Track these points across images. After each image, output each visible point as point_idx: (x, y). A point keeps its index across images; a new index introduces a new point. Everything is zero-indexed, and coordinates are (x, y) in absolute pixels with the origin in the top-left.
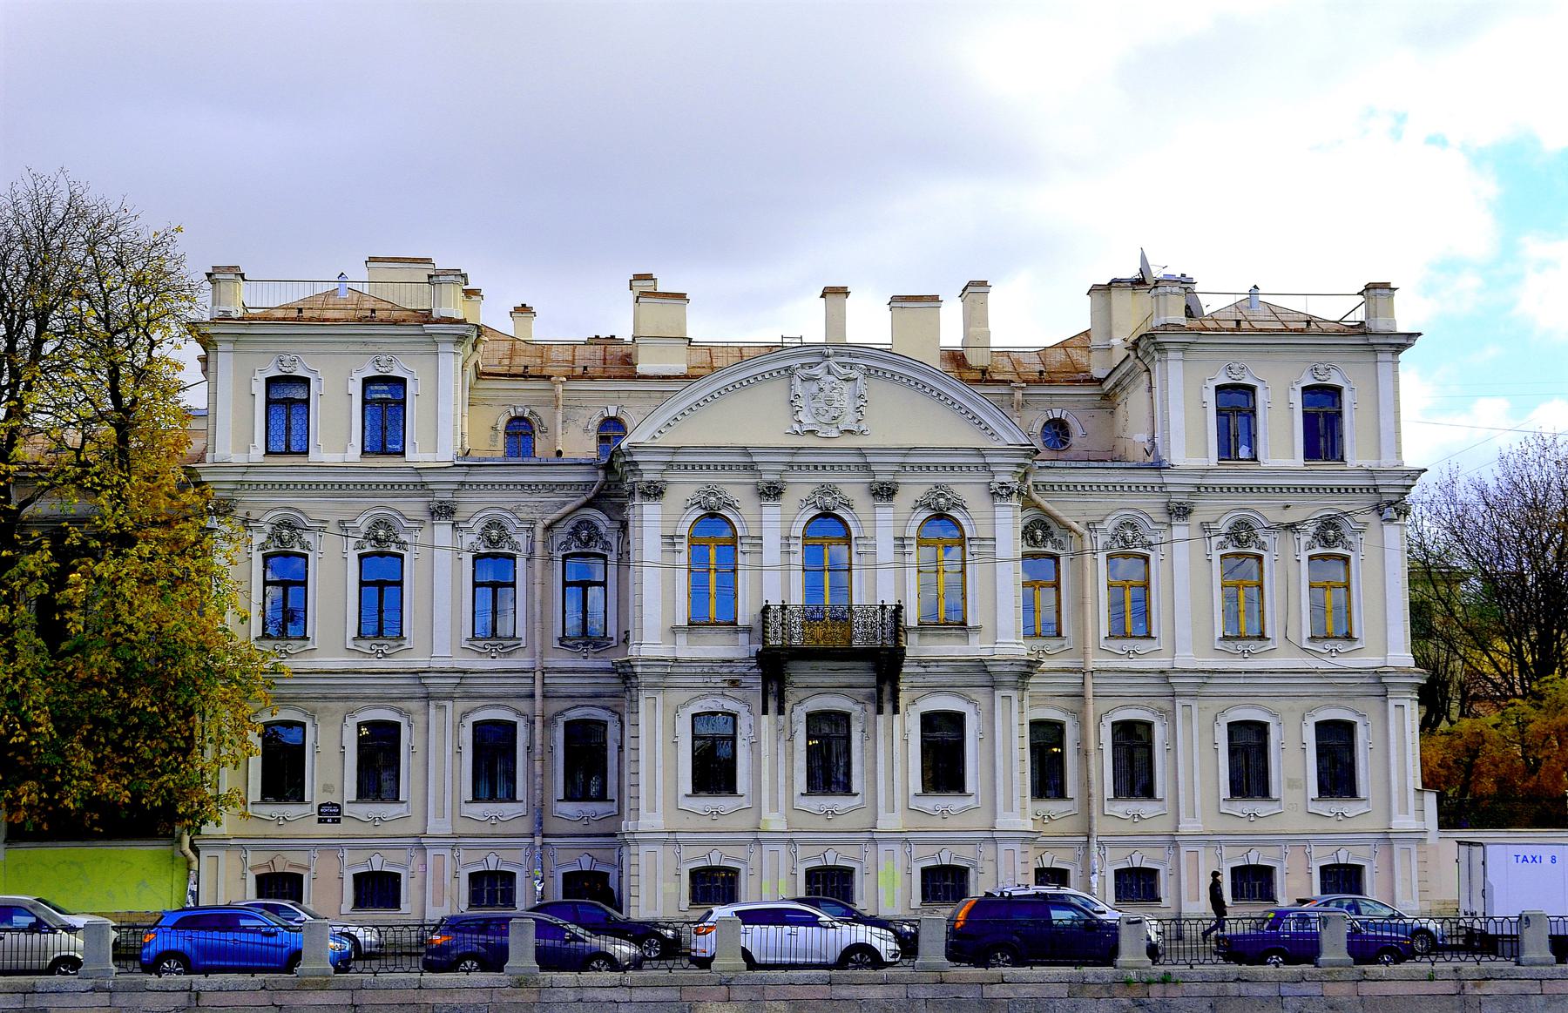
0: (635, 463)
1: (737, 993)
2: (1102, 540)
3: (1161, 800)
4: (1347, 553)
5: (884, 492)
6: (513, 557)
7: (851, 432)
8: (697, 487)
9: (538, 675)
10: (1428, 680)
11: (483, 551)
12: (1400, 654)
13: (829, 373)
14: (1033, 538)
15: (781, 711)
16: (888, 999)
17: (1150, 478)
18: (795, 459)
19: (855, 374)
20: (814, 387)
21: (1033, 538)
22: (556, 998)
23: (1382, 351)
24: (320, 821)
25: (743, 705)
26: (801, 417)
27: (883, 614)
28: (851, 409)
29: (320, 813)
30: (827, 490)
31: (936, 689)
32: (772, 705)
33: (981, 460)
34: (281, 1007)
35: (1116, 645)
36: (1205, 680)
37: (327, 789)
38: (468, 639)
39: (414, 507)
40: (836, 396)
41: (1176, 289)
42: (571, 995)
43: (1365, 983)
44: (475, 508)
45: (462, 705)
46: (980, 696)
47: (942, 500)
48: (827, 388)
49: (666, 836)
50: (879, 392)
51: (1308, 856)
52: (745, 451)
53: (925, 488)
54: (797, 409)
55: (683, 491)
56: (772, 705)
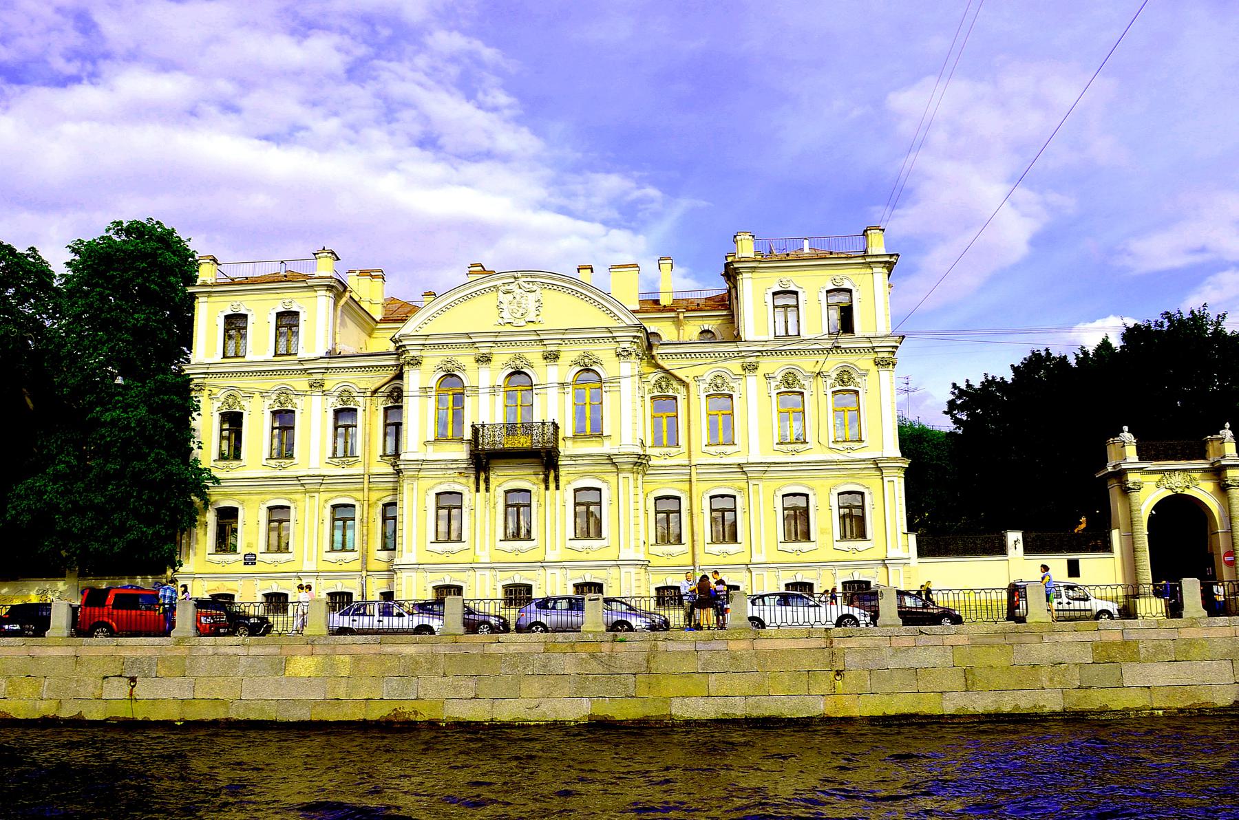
0: (404, 346)
1: (318, 649)
2: (703, 386)
3: (740, 543)
4: (857, 389)
6: (355, 410)
7: (532, 322)
8: (442, 358)
9: (366, 477)
10: (909, 465)
12: (892, 448)
13: (520, 288)
14: (660, 387)
15: (487, 490)
16: (419, 655)
17: (731, 347)
18: (497, 339)
19: (535, 288)
20: (510, 296)
21: (660, 387)
22: (200, 653)
23: (875, 267)
24: (245, 564)
25: (464, 485)
27: (544, 428)
28: (534, 308)
29: (245, 559)
31: (584, 475)
32: (482, 486)
33: (610, 335)
34: (33, 657)
35: (713, 449)
36: (766, 468)
37: (249, 545)
38: (329, 458)
39: (301, 383)
40: (523, 301)
41: (747, 237)
42: (210, 651)
43: (759, 641)
44: (332, 382)
45: (324, 496)
46: (612, 478)
47: (586, 360)
48: (518, 297)
49: (417, 566)
50: (549, 297)
51: (834, 575)
52: (468, 335)
53: (578, 353)
54: (501, 310)
55: (433, 362)
56: (482, 486)
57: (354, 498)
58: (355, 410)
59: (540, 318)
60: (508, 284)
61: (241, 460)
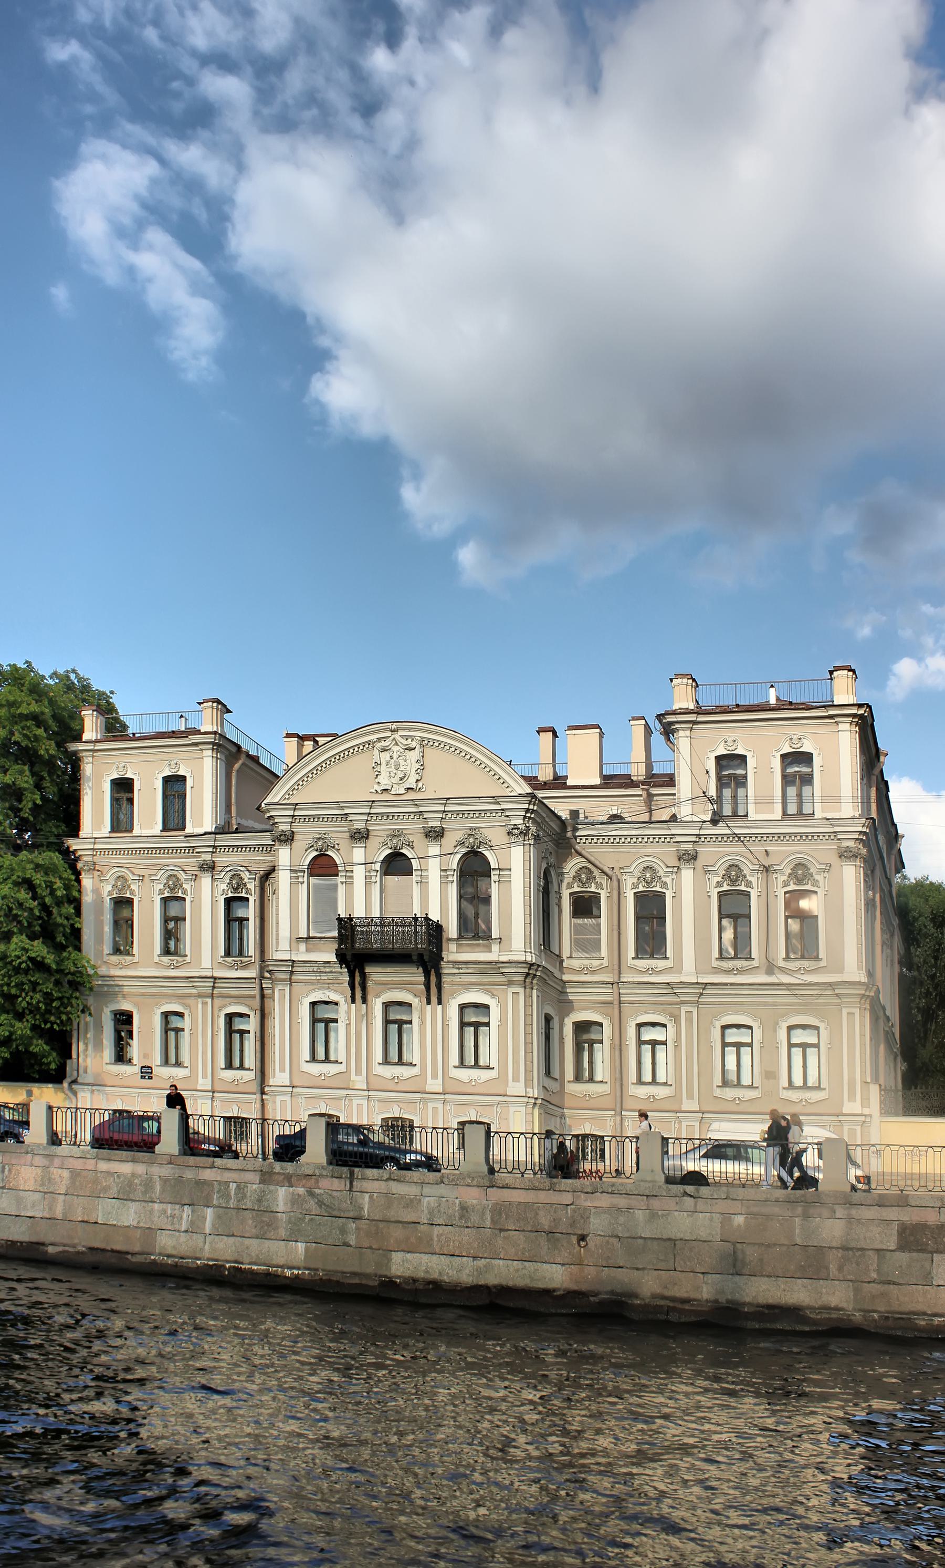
5: (436, 834)
6: (247, 899)
11: (230, 895)
13: (396, 744)
19: (414, 744)
20: (385, 756)
26: (380, 779)
30: (396, 834)
31: (469, 986)
39: (191, 862)
40: (402, 762)
45: (218, 1002)
48: (395, 756)
57: (248, 1006)
58: (247, 899)
59: (420, 785)
60: (385, 739)
61: (133, 955)
